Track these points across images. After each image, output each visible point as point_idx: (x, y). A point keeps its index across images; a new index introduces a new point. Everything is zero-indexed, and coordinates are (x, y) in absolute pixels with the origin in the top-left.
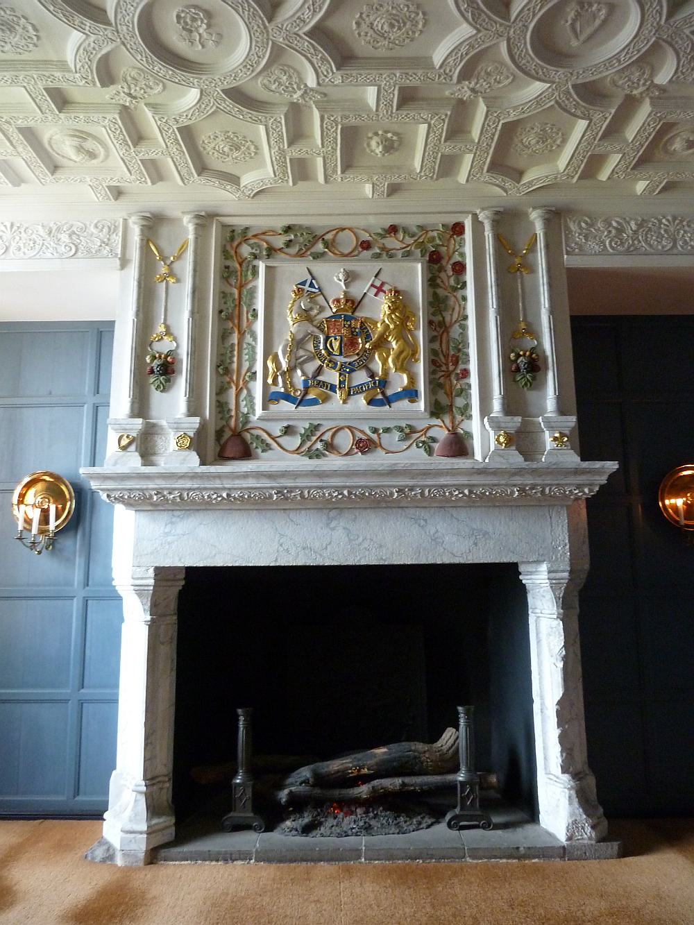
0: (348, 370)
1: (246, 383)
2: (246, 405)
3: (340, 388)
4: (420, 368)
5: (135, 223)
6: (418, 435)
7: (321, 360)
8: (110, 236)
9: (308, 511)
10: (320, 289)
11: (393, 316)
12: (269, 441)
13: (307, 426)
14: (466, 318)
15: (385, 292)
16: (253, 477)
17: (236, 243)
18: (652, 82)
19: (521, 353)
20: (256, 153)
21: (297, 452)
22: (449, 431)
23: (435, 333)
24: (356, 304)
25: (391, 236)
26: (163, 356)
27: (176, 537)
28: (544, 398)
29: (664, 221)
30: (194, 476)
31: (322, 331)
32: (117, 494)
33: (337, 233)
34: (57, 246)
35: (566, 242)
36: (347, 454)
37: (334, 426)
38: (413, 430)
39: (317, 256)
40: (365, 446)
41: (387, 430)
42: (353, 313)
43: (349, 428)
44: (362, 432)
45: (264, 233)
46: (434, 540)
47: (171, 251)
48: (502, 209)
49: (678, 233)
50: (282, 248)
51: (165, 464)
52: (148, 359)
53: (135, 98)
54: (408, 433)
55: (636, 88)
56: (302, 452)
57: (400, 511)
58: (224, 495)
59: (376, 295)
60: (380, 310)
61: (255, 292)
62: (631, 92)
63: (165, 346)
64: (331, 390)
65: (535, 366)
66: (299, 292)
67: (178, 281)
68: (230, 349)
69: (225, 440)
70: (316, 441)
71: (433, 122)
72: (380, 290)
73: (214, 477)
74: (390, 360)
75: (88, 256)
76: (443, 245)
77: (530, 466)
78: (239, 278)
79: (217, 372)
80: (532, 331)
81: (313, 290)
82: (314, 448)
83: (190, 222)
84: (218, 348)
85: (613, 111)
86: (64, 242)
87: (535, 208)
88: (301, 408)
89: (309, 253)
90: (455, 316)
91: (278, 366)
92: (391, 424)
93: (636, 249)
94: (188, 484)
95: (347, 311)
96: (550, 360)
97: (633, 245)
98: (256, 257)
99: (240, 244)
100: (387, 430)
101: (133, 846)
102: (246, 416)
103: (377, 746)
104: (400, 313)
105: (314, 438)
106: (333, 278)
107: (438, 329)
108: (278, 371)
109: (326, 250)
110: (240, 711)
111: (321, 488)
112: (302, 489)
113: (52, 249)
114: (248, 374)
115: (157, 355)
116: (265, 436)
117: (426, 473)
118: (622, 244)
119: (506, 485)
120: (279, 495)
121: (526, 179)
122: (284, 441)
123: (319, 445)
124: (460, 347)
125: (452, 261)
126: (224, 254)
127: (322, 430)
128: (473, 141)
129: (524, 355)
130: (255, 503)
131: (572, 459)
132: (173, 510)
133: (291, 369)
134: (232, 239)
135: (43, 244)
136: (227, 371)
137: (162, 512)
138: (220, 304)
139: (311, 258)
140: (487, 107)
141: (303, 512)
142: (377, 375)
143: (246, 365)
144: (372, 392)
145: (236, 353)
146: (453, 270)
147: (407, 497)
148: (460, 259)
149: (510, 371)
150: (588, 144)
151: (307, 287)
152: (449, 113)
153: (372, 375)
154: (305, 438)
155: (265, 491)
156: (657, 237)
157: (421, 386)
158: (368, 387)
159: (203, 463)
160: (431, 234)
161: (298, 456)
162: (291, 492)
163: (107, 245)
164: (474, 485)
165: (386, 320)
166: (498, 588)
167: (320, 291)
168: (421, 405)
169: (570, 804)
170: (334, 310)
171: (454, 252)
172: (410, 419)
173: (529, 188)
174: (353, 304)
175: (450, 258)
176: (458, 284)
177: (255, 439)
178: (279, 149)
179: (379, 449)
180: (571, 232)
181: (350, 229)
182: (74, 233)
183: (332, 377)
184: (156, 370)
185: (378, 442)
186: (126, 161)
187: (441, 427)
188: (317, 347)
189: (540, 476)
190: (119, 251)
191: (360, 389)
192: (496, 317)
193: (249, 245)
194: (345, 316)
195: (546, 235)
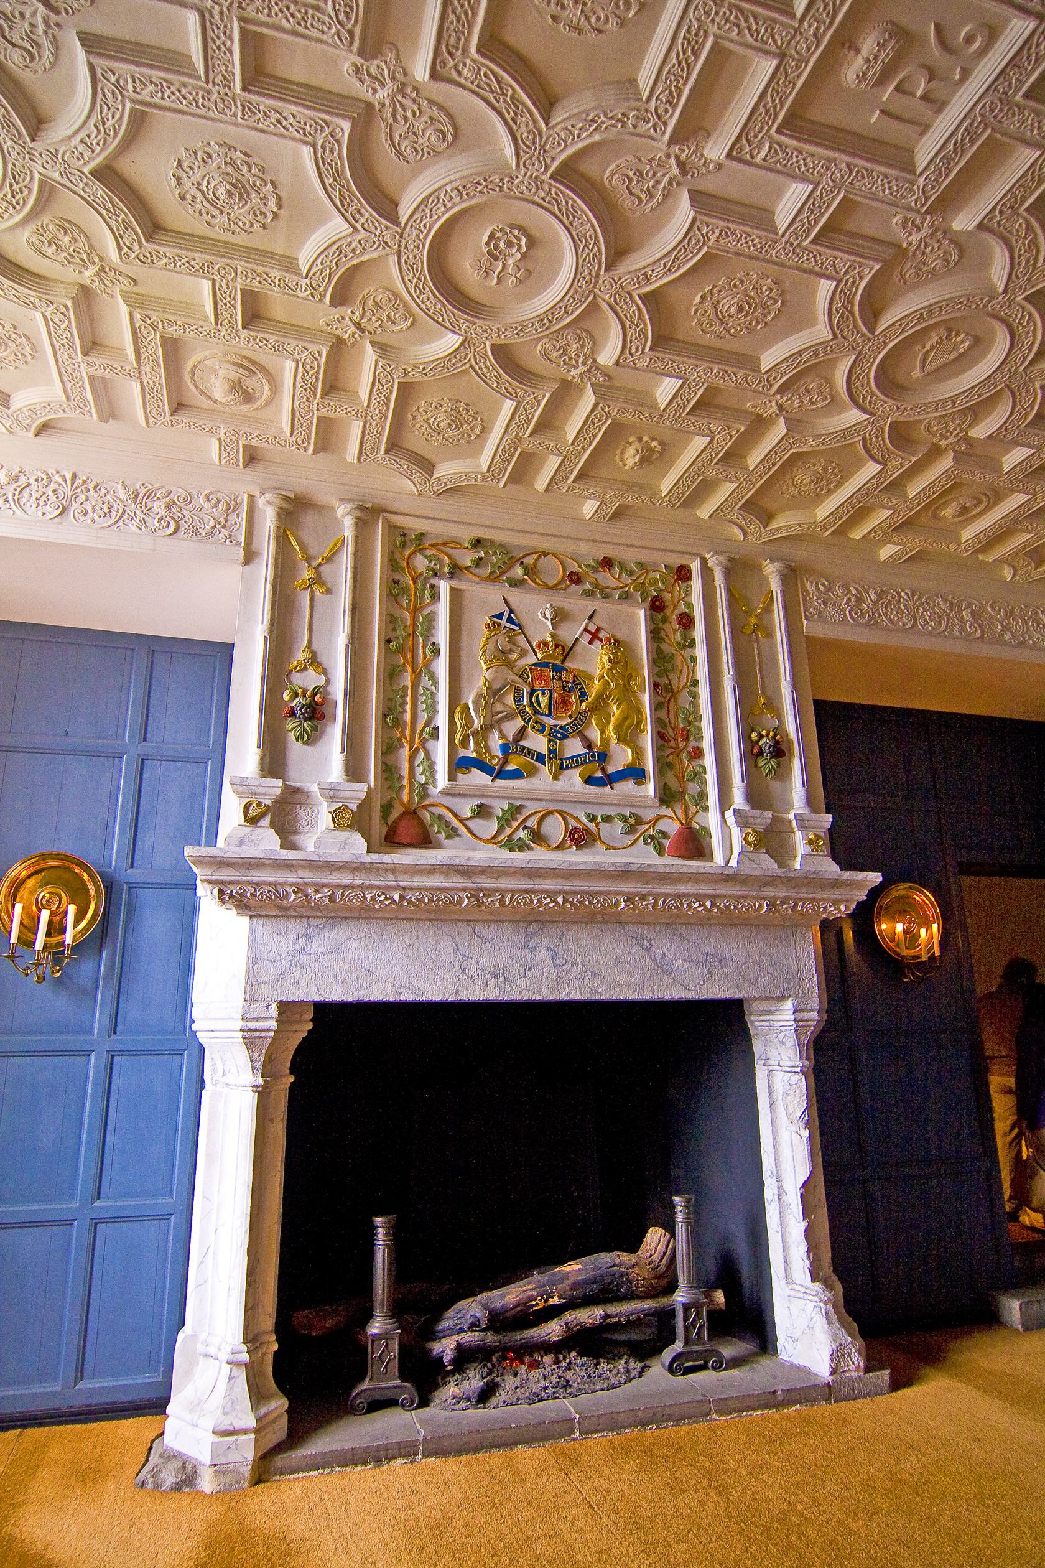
1: (423, 742)
3: (550, 758)
4: (647, 741)
5: (269, 503)
6: (645, 827)
12: (456, 823)
13: (506, 807)
14: (696, 683)
15: (601, 640)
17: (407, 553)
19: (764, 733)
23: (661, 699)
28: (788, 791)
30: (357, 867)
32: (235, 890)
33: (539, 557)
36: (558, 848)
38: (639, 821)
39: (515, 583)
40: (580, 838)
41: (608, 819)
42: (563, 661)
43: (560, 812)
44: (576, 819)
45: (445, 544)
47: (321, 552)
52: (286, 696)
53: (362, 330)
54: (633, 824)
58: (396, 897)
59: (590, 643)
60: (596, 662)
63: (310, 680)
65: (780, 751)
66: (494, 626)
67: (329, 591)
72: (595, 636)
74: (611, 727)
75: (195, 538)
82: (515, 837)
88: (499, 782)
93: (877, 622)
94: (346, 879)
97: (873, 617)
100: (608, 819)
101: (234, 1456)
102: (424, 788)
103: (563, 1262)
105: (515, 824)
110: (379, 1221)
112: (503, 892)
116: (450, 817)
117: (665, 877)
119: (754, 898)
121: (774, 525)
122: (476, 824)
123: (522, 834)
125: (677, 612)
126: (392, 563)
127: (526, 813)
128: (746, 468)
129: (767, 735)
131: (831, 868)
133: (487, 728)
135: (124, 512)
136: (398, 723)
137: (293, 920)
143: (423, 717)
144: (589, 766)
145: (409, 699)
146: (679, 622)
148: (686, 610)
149: (751, 753)
151: (503, 622)
153: (589, 746)
154: (503, 822)
157: (649, 766)
159: (368, 851)
163: (224, 527)
164: (718, 896)
166: (713, 1032)
167: (521, 628)
168: (650, 789)
169: (829, 1323)
170: (540, 656)
178: (516, 437)
180: (808, 594)
183: (539, 743)
187: (672, 818)
188: (519, 701)
191: (576, 761)
193: (426, 557)
195: (783, 593)
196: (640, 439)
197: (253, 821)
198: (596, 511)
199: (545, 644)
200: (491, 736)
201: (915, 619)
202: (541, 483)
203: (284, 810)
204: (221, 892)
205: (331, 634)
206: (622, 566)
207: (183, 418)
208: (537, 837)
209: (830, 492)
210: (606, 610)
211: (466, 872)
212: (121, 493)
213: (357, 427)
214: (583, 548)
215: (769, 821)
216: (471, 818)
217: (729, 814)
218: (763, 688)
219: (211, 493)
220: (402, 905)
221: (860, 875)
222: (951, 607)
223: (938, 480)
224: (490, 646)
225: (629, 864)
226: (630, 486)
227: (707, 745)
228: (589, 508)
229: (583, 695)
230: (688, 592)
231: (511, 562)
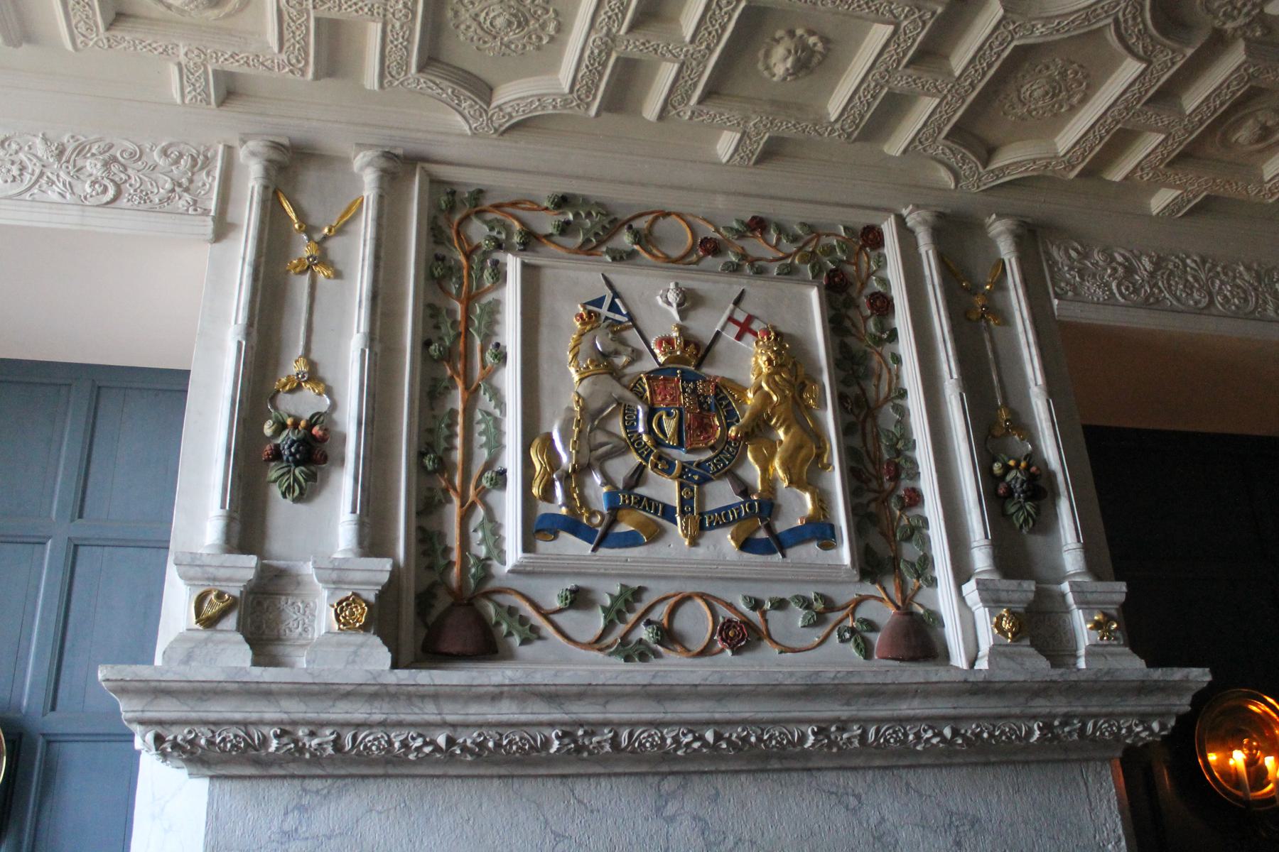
0: (696, 477)
1: (482, 493)
2: (484, 541)
3: (683, 513)
5: (253, 154)
7: (640, 455)
8: (193, 174)
9: (613, 779)
10: (630, 316)
11: (777, 378)
12: (537, 619)
13: (617, 590)
14: (903, 394)
15: (755, 334)
16: (512, 697)
17: (457, 217)
18: (1262, 11)
19: (1012, 463)
20: (552, 39)
21: (597, 646)
22: (898, 607)
23: (852, 418)
24: (702, 352)
25: (755, 237)
26: (303, 423)
27: (309, 843)
28: (1057, 548)
29: (1188, 261)
30: (378, 694)
31: (641, 396)
32: (181, 734)
33: (656, 219)
34: (74, 182)
35: (1052, 278)
36: (705, 652)
37: (672, 592)
38: (830, 605)
39: (621, 257)
40: (740, 635)
41: (780, 604)
42: (698, 366)
43: (702, 596)
44: (730, 606)
45: (514, 204)
46: (879, 839)
47: (325, 220)
49: (1213, 284)
50: (551, 235)
51: (308, 662)
52: (268, 429)
55: (1234, 19)
56: (609, 647)
57: (805, 775)
58: (441, 740)
59: (739, 337)
60: (750, 365)
61: (498, 312)
62: (1224, 24)
63: (306, 403)
64: (664, 516)
65: (1039, 488)
66: (590, 319)
67: (338, 275)
68: (447, 420)
69: (438, 614)
70: (636, 624)
71: (905, 23)
72: (745, 328)
73: (423, 697)
74: (777, 463)
75: (142, 206)
76: (848, 262)
77: (1066, 677)
78: (465, 280)
79: (421, 467)
81: (618, 317)
82: (634, 637)
83: (369, 164)
84: (420, 416)
85: (1189, 52)
86: (91, 175)
87: (1000, 216)
88: (603, 551)
89: (604, 249)
90: (884, 388)
92: (786, 592)
93: (1157, 301)
94: (358, 712)
95: (687, 363)
96: (1060, 478)
97: (1152, 294)
98: (499, 246)
99: (466, 218)
100: (780, 604)
102: (484, 564)
104: (790, 372)
105: (632, 618)
106: (657, 302)
107: (856, 411)
108: (553, 471)
109: (636, 247)
112: (615, 726)
113: (61, 185)
114: (488, 474)
115: (289, 421)
116: (527, 610)
117: (876, 693)
118: (1136, 291)
120: (566, 741)
121: (997, 164)
122: (568, 620)
124: (900, 446)
125: (868, 291)
126: (435, 233)
127: (648, 599)
128: (950, 73)
129: (1017, 465)
130: (510, 760)
131: (1132, 666)
132: (304, 777)
133: (582, 470)
135: (42, 174)
136: (444, 466)
137: (277, 783)
138: (424, 330)
139: (609, 259)
140: (1005, 11)
141: (604, 782)
142: (754, 491)
143: (482, 455)
144: (747, 524)
145: (459, 429)
146: (872, 306)
147: (832, 743)
149: (996, 496)
150: (1126, 108)
151: (604, 311)
152: (940, 10)
154: (613, 615)
155: (533, 731)
156: (1185, 286)
158: (739, 514)
159: (395, 665)
160: (825, 240)
161: (600, 655)
162: (593, 734)
163: (187, 190)
165: (764, 385)
168: (844, 554)
170: (662, 359)
171: (869, 276)
172: (828, 582)
173: (998, 178)
174: (699, 351)
175: (864, 285)
176: (883, 332)
177: (506, 615)
178: (607, 34)
179: (766, 643)
180: (1056, 263)
181: (679, 215)
182: (114, 159)
183: (667, 490)
184: (274, 456)
185: (763, 628)
186: (286, 17)
187: (881, 600)
188: (630, 426)
190: (213, 205)
191: (722, 518)
192: (961, 395)
193: (486, 222)
194: (683, 372)
196: (791, 33)
197: (209, 623)
198: (736, 150)
199: (669, 341)
200: (588, 481)
201: (1210, 294)
202: (651, 109)
203: (259, 603)
204: (159, 739)
205: (342, 332)
206: (781, 229)
207: (125, 34)
208: (669, 636)
209: (1073, 110)
210: (762, 296)
211: (552, 696)
212: (40, 149)
213: (375, 30)
214: (720, 203)
215: (1031, 596)
216: (560, 611)
217: (970, 588)
218: (1005, 398)
219: (170, 145)
220: (453, 755)
221: (1177, 674)
222: (1259, 278)
223: (1226, 83)
224: (584, 347)
225: (817, 673)
226: (780, 106)
227: (928, 483)
228: (725, 144)
229: (730, 418)
230: (882, 262)
231: (614, 226)
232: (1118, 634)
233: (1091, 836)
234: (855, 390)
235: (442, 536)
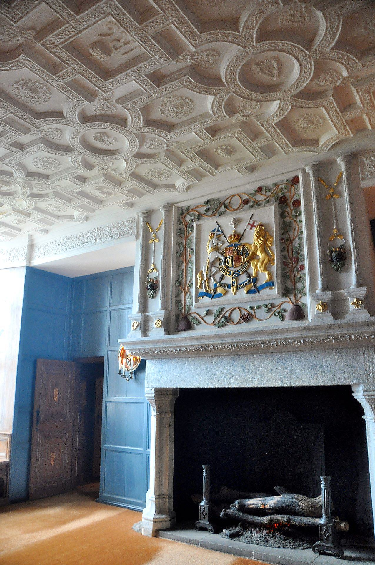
3: (233, 286)
6: (276, 308)
12: (200, 319)
14: (302, 233)
22: (293, 304)
23: (285, 245)
30: (163, 341)
36: (238, 323)
38: (273, 305)
39: (221, 214)
40: (247, 318)
41: (259, 307)
44: (246, 310)
45: (197, 207)
48: (317, 163)
54: (270, 307)
59: (251, 229)
72: (253, 226)
76: (288, 192)
80: (341, 234)
81: (219, 233)
82: (221, 321)
88: (213, 300)
91: (202, 278)
100: (259, 307)
105: (221, 316)
111: (223, 344)
116: (198, 317)
123: (223, 320)
126: (179, 221)
127: (225, 310)
133: (209, 279)
134: (182, 214)
136: (180, 284)
148: (298, 198)
149: (327, 262)
160: (280, 187)
164: (307, 337)
168: (275, 290)
171: (294, 195)
174: (239, 237)
175: (292, 199)
179: (255, 319)
181: (238, 195)
183: (228, 279)
184: (150, 288)
187: (289, 302)
189: (345, 329)
191: (244, 285)
195: (347, 170)
218: (337, 225)
227: (306, 263)
232: (362, 305)
233: (363, 371)
234: (287, 236)
235: (180, 301)
